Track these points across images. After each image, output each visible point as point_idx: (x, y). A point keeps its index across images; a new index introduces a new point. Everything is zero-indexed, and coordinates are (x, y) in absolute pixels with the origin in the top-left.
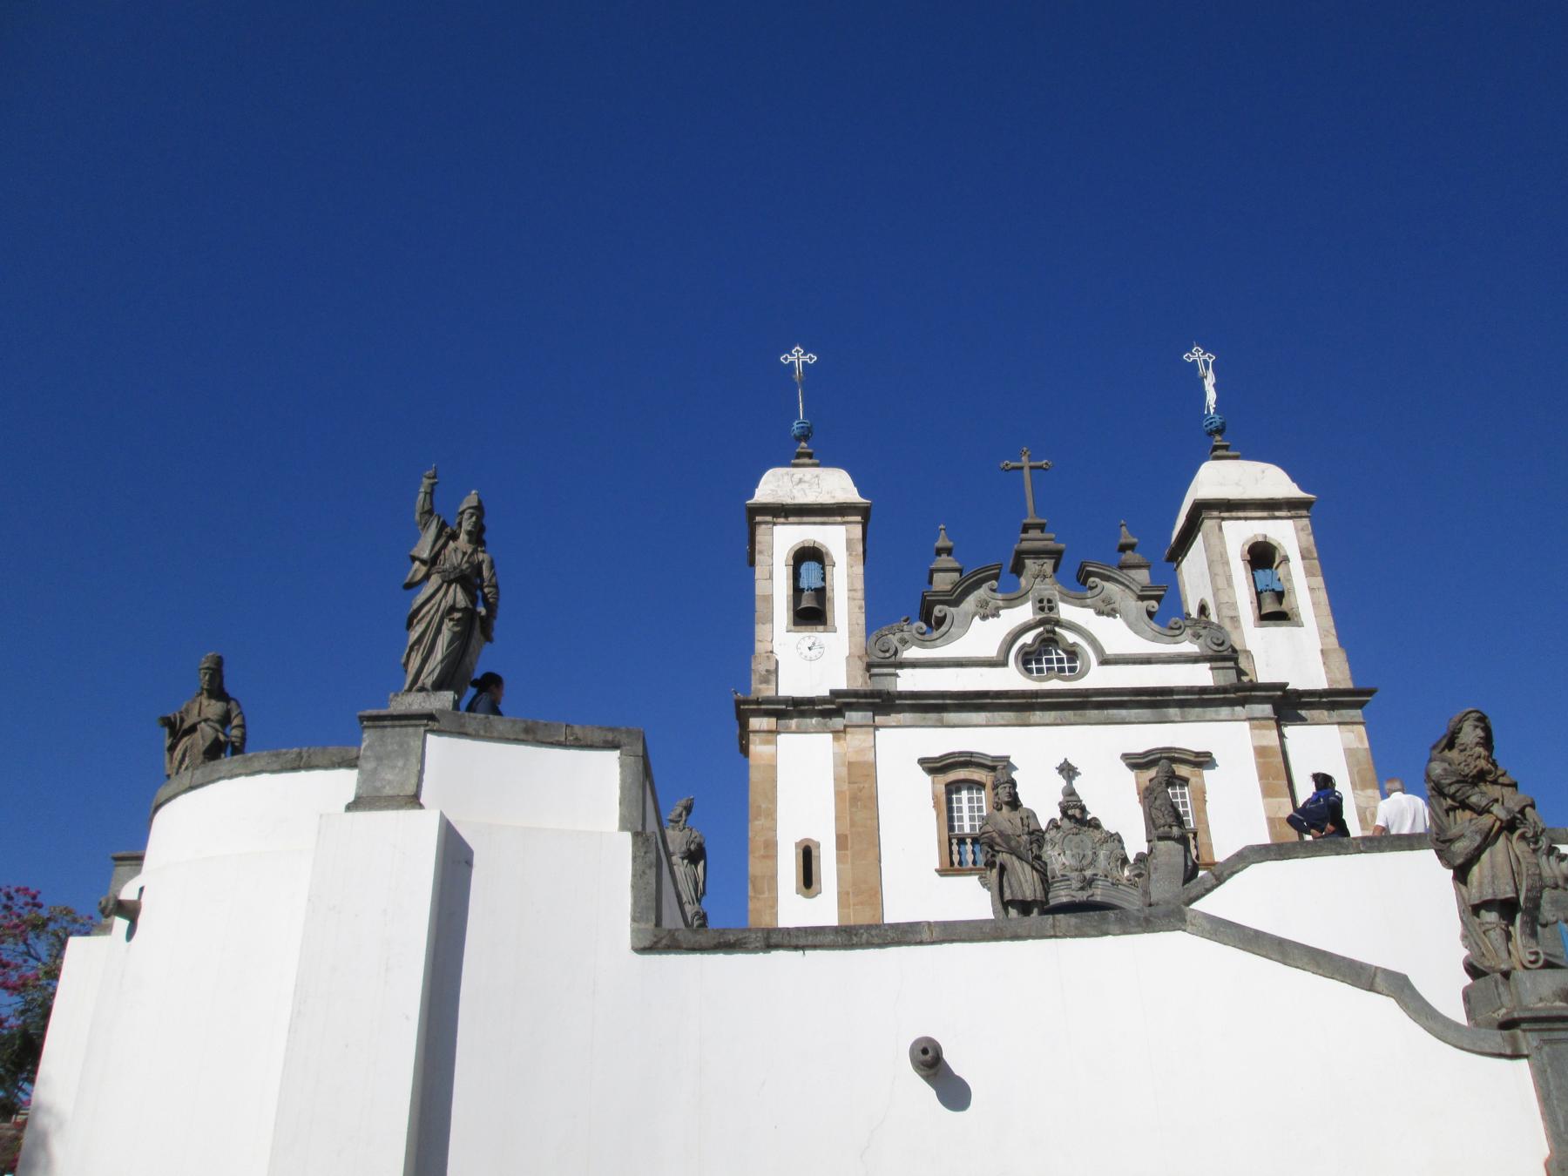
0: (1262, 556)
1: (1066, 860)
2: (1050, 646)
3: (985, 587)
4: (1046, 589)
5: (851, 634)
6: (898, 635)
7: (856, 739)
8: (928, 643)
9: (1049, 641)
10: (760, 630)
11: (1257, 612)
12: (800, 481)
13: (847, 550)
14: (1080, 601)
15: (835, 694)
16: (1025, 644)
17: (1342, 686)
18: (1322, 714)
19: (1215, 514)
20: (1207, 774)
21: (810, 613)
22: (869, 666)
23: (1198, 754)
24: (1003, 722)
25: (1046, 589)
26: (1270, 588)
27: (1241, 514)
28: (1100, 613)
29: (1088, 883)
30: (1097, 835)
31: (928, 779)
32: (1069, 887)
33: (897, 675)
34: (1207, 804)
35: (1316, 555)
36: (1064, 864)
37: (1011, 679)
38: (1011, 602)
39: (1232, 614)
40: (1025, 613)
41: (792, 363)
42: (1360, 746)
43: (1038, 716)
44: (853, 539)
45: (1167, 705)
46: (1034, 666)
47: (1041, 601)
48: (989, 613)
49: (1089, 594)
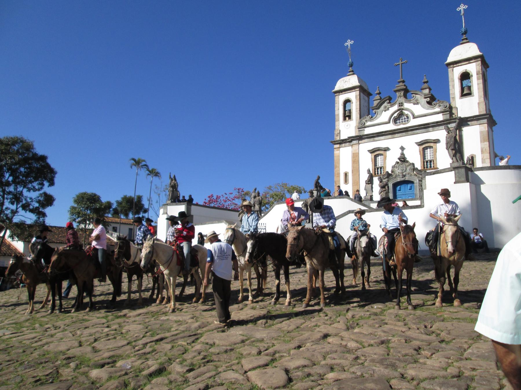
0: (465, 76)
1: (400, 171)
3: (386, 102)
5: (356, 120)
6: (365, 119)
7: (355, 147)
9: (401, 114)
10: (337, 123)
12: (346, 81)
14: (409, 102)
15: (349, 138)
17: (482, 113)
18: (475, 122)
19: (452, 66)
20: (438, 144)
21: (347, 116)
22: (359, 128)
23: (434, 140)
27: (460, 64)
28: (414, 104)
29: (404, 176)
30: (407, 164)
31: (370, 154)
32: (400, 177)
33: (364, 130)
35: (481, 73)
37: (391, 127)
38: (392, 106)
40: (396, 108)
41: (348, 45)
43: (397, 135)
45: (429, 127)
46: (398, 121)
47: (400, 104)
48: (387, 109)
49: (412, 99)
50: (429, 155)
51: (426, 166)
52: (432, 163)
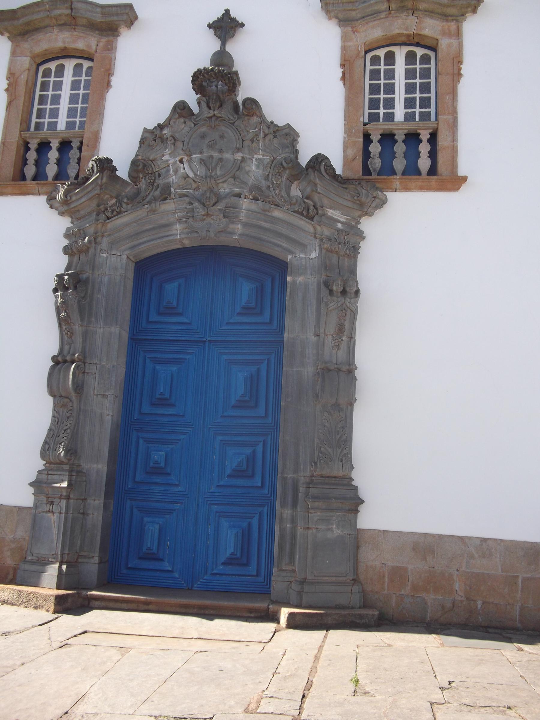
34: (462, 80)
50: (400, 96)
51: (376, 163)
52: (424, 148)
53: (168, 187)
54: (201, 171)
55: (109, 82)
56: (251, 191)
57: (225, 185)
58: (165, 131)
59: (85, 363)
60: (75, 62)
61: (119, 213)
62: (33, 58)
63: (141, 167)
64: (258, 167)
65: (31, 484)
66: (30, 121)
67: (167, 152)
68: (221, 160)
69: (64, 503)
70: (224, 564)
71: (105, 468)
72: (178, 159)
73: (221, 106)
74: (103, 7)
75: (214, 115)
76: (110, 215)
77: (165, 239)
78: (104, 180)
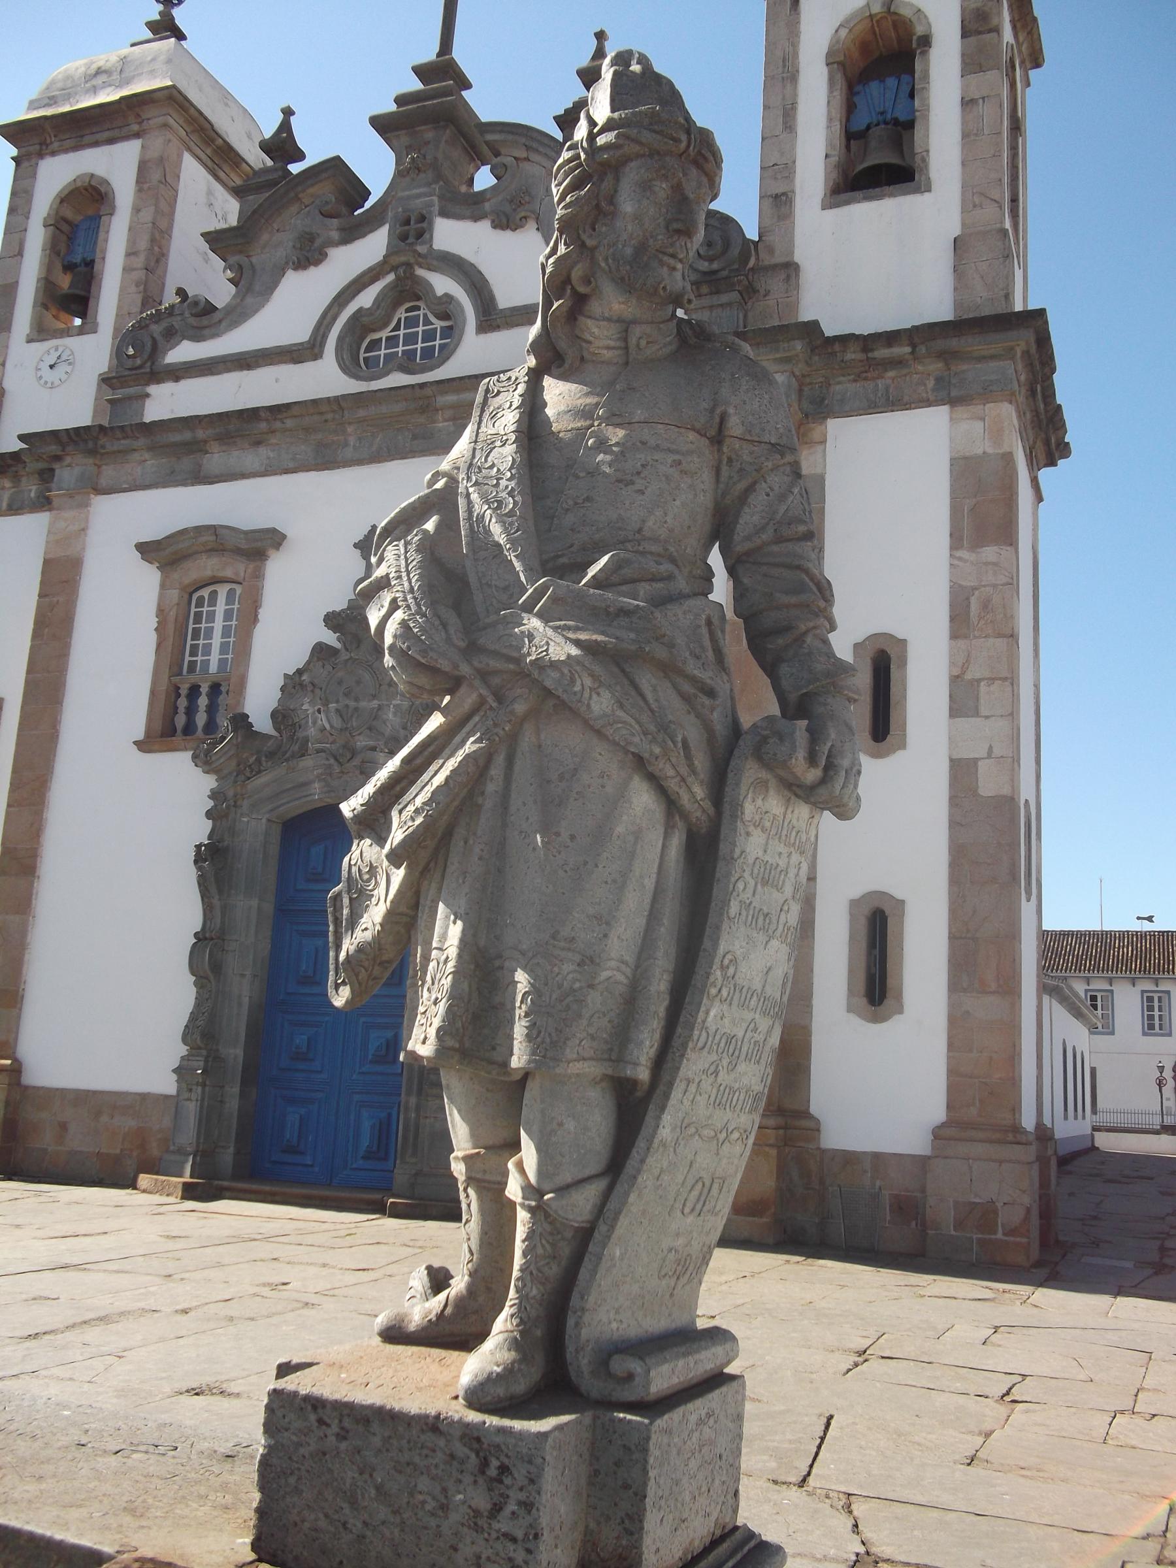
2: (418, 308)
4: (418, 196)
6: (164, 324)
8: (206, 332)
11: (834, 175)
13: (137, 182)
16: (360, 310)
24: (291, 465)
25: (418, 196)
26: (889, 116)
33: (148, 395)
36: (323, 729)
38: (353, 232)
39: (780, 190)
42: (990, 450)
44: (149, 161)
53: (306, 740)
54: (337, 722)
55: (256, 616)
56: (386, 744)
57: (361, 738)
58: (304, 678)
59: (224, 940)
60: (227, 587)
61: (259, 772)
62: (183, 589)
63: (280, 719)
64: (395, 714)
65: (174, 1071)
66: (183, 660)
67: (307, 700)
68: (356, 709)
69: (200, 1089)
70: (363, 1158)
71: (242, 1054)
72: (316, 708)
73: (358, 647)
74: (246, 533)
75: (351, 658)
76: (249, 775)
77: (304, 800)
78: (239, 739)
